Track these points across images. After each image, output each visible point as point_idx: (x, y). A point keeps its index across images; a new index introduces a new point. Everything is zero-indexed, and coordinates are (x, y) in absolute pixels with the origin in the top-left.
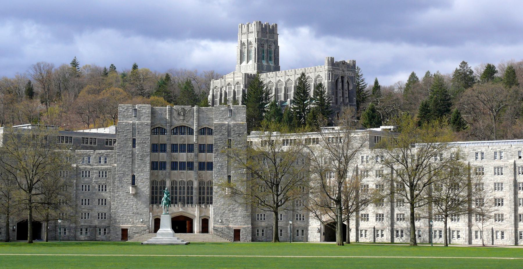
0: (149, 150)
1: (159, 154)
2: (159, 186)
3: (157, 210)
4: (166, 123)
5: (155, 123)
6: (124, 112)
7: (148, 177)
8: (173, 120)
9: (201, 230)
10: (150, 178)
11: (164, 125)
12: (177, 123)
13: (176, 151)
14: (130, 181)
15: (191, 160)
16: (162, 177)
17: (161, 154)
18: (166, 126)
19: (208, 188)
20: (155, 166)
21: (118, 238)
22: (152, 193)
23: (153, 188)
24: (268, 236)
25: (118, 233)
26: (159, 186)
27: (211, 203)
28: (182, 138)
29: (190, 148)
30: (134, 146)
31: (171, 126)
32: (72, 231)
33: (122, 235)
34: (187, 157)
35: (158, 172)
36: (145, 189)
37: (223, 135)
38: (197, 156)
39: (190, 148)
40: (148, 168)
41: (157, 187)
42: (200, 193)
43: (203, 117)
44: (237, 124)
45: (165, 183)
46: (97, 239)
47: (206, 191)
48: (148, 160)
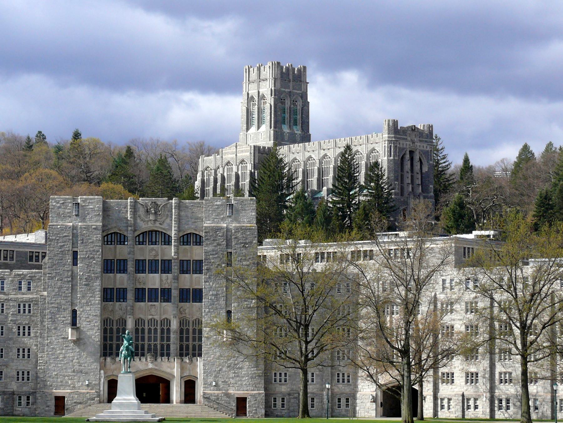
0: (99, 269)
1: (115, 277)
2: (115, 328)
3: (113, 367)
4: (127, 227)
5: (109, 227)
6: (59, 207)
7: (98, 313)
8: (138, 221)
9: (183, 398)
10: (101, 315)
11: (124, 229)
12: (144, 226)
13: (143, 271)
14: (69, 320)
15: (167, 286)
16: (121, 313)
17: (119, 275)
18: (127, 230)
19: (194, 330)
20: (110, 295)
21: (49, 411)
22: (105, 339)
23: (105, 331)
24: (292, 408)
25: (49, 404)
26: (115, 328)
27: (200, 355)
28: (153, 249)
29: (165, 266)
30: (75, 263)
31: (135, 230)
33: (56, 406)
34: (161, 280)
35: (114, 306)
37: (219, 244)
38: (176, 279)
39: (165, 266)
41: (111, 330)
42: (181, 339)
43: (186, 216)
44: (241, 228)
45: (125, 322)
46: (15, 413)
47: (191, 335)
48: (97, 285)
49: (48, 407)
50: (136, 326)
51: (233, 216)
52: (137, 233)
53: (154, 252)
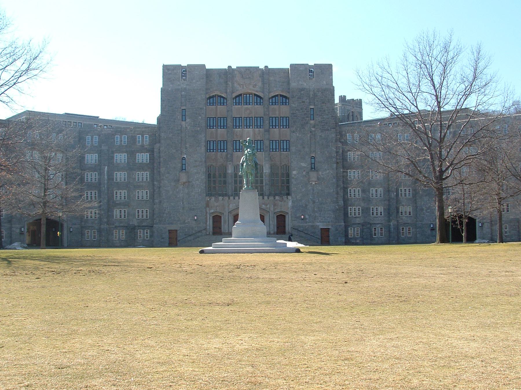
7: (204, 160)
9: (276, 230)
10: (205, 162)
15: (259, 138)
17: (219, 130)
20: (212, 146)
23: (209, 176)
24: (365, 237)
27: (288, 194)
28: (247, 109)
32: (104, 234)
36: (199, 179)
38: (268, 131)
40: (203, 149)
41: (215, 175)
43: (275, 81)
45: (225, 168)
48: (202, 138)
49: (163, 238)
50: (234, 171)
51: (314, 79)
52: (234, 95)
53: (248, 111)
